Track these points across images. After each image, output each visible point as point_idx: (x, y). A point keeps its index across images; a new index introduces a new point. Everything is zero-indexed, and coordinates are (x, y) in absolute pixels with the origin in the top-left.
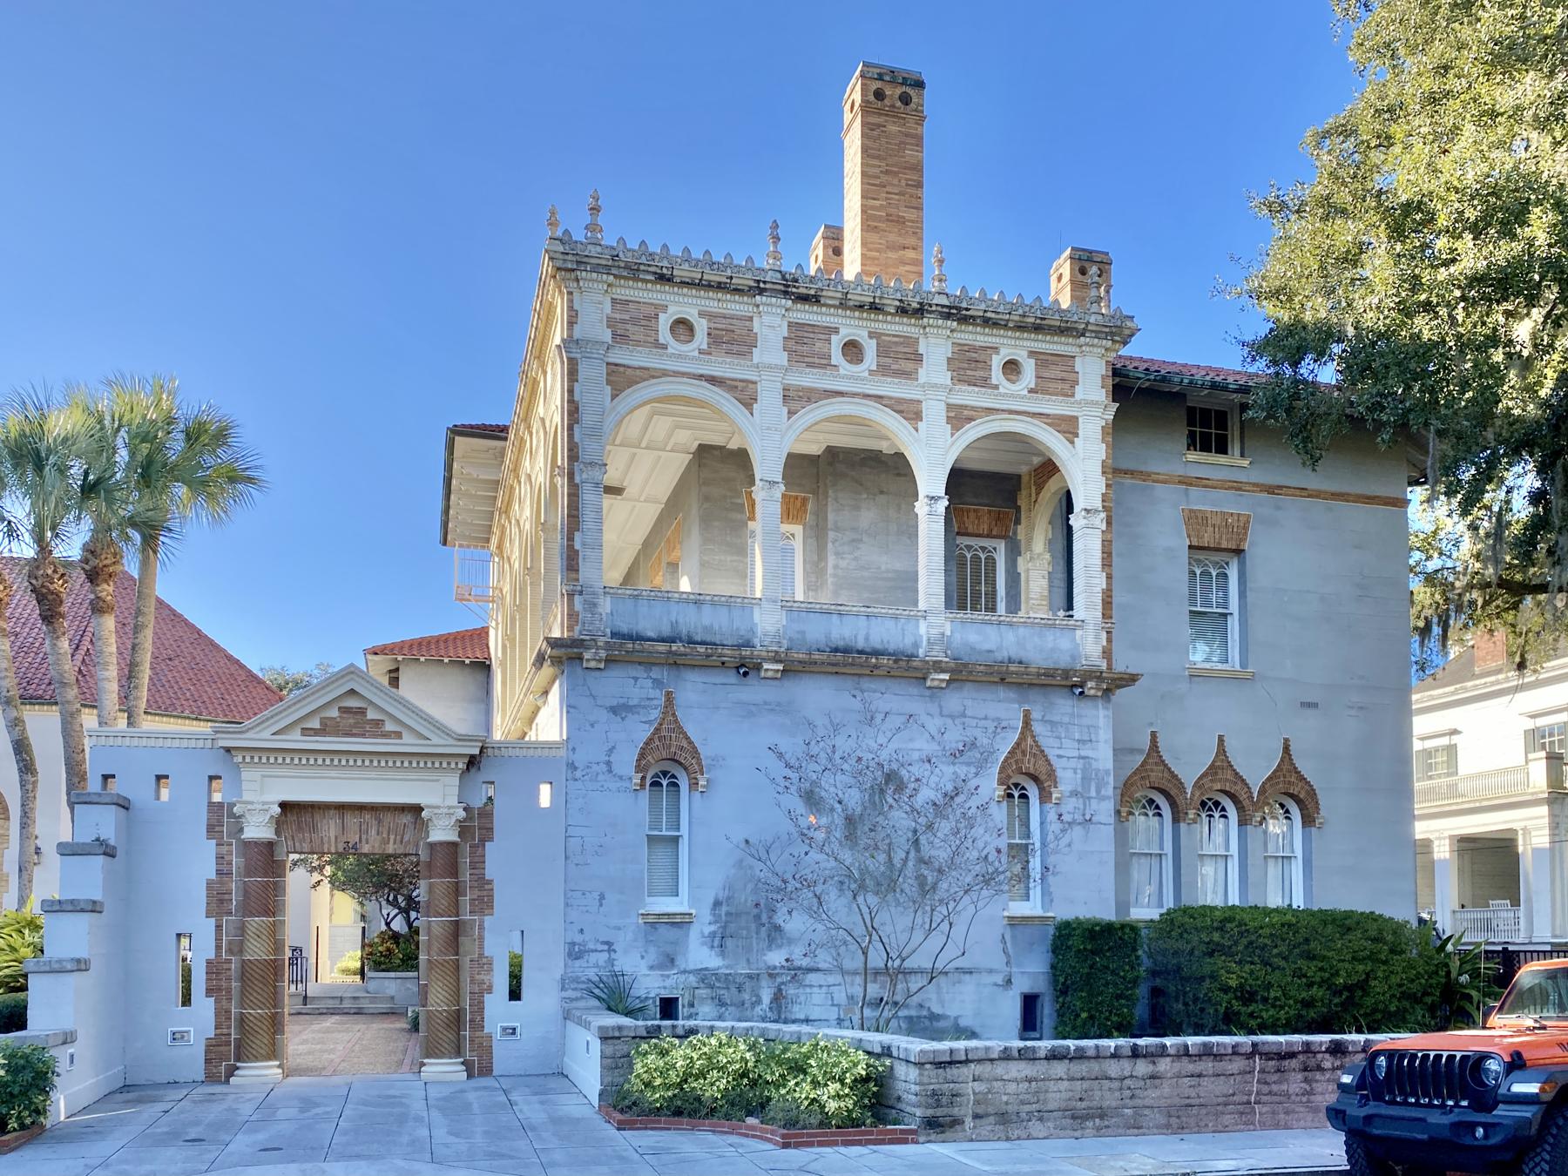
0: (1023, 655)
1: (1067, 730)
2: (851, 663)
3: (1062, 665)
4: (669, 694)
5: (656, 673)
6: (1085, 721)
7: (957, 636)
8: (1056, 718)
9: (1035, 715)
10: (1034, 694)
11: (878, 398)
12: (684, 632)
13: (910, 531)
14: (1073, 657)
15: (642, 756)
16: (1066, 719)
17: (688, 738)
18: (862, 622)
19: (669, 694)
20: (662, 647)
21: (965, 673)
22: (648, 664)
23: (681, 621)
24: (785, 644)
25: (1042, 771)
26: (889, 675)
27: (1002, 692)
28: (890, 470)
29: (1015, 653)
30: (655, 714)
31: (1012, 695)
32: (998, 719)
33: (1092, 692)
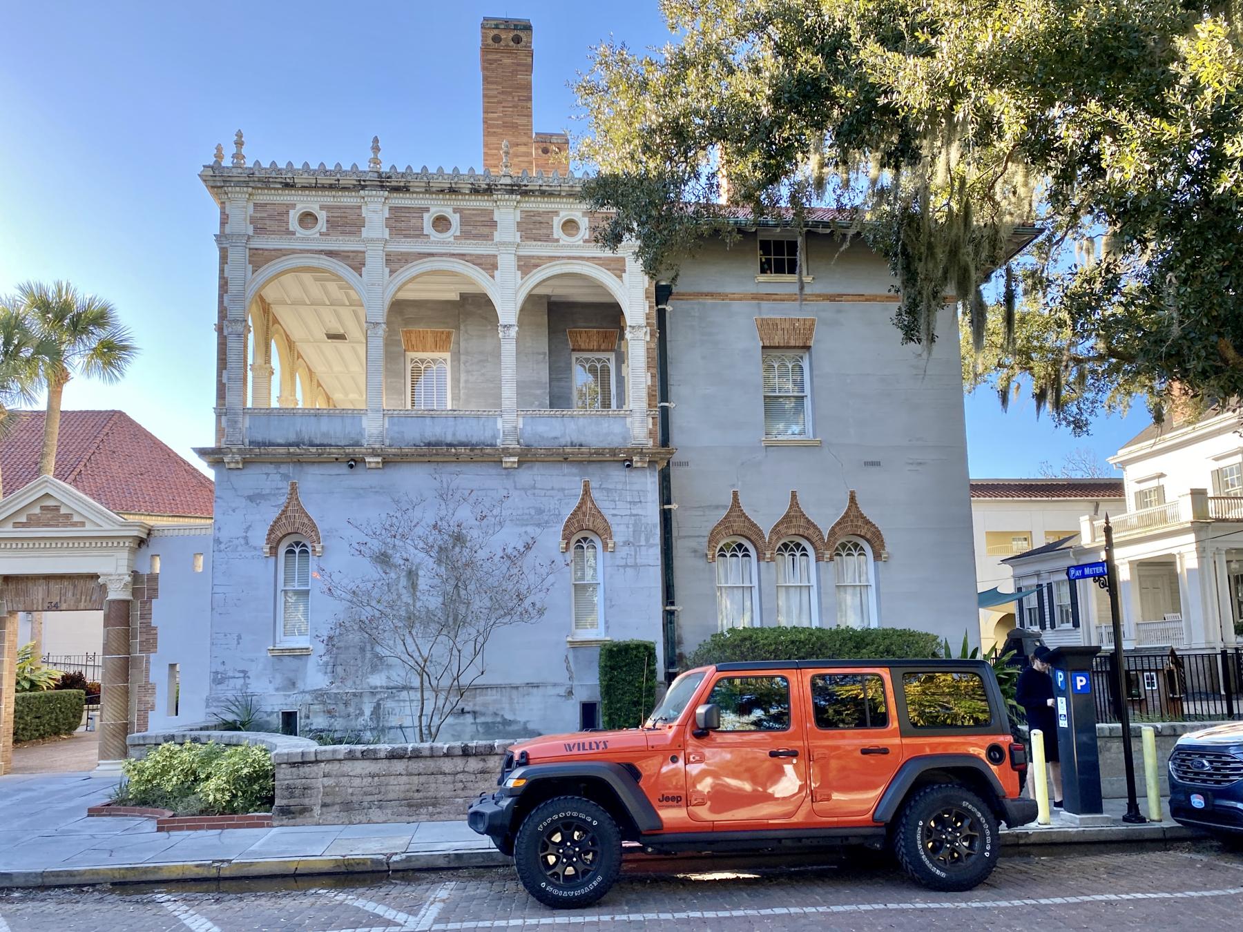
0: (582, 439)
1: (620, 495)
2: (436, 453)
3: (614, 445)
4: (293, 484)
5: (284, 469)
6: (636, 487)
7: (529, 428)
8: (610, 486)
9: (593, 484)
10: (591, 469)
11: (462, 256)
12: (306, 438)
13: (497, 354)
14: (625, 439)
15: (272, 531)
16: (619, 486)
17: (308, 516)
18: (451, 422)
19: (293, 484)
20: (282, 450)
21: (528, 456)
22: (277, 463)
23: (304, 428)
24: (387, 442)
25: (599, 524)
26: (472, 461)
27: (566, 468)
28: (475, 307)
29: (576, 438)
30: (283, 500)
31: (574, 470)
32: (563, 490)
33: (639, 465)
